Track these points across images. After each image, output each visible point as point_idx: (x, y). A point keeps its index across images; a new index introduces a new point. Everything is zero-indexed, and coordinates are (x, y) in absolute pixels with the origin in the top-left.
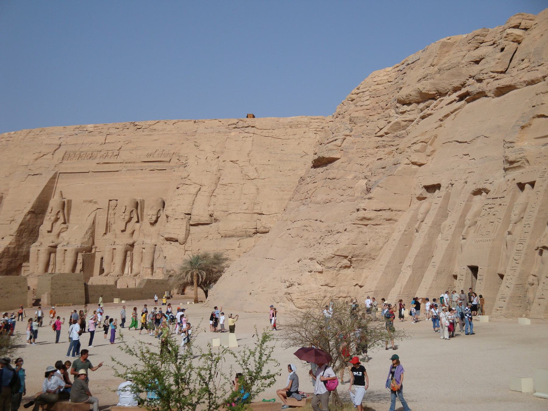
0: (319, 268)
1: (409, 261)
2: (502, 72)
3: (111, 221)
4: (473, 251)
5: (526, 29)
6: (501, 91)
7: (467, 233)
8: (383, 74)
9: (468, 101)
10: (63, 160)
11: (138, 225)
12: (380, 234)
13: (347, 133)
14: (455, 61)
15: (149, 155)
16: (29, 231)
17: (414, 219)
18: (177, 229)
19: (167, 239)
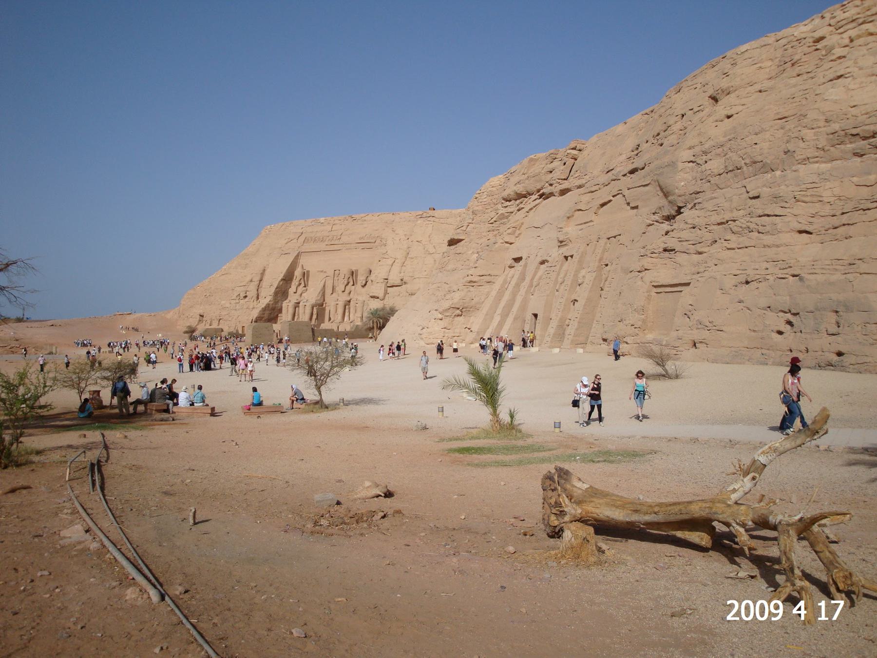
0: (440, 316)
1: (499, 311)
2: (566, 179)
3: (336, 284)
4: (536, 304)
6: (563, 192)
7: (534, 291)
8: (496, 180)
9: (545, 199)
13: (470, 221)
14: (537, 171)
15: (360, 239)
16: (282, 293)
17: (505, 282)
18: (378, 290)
19: (372, 297)
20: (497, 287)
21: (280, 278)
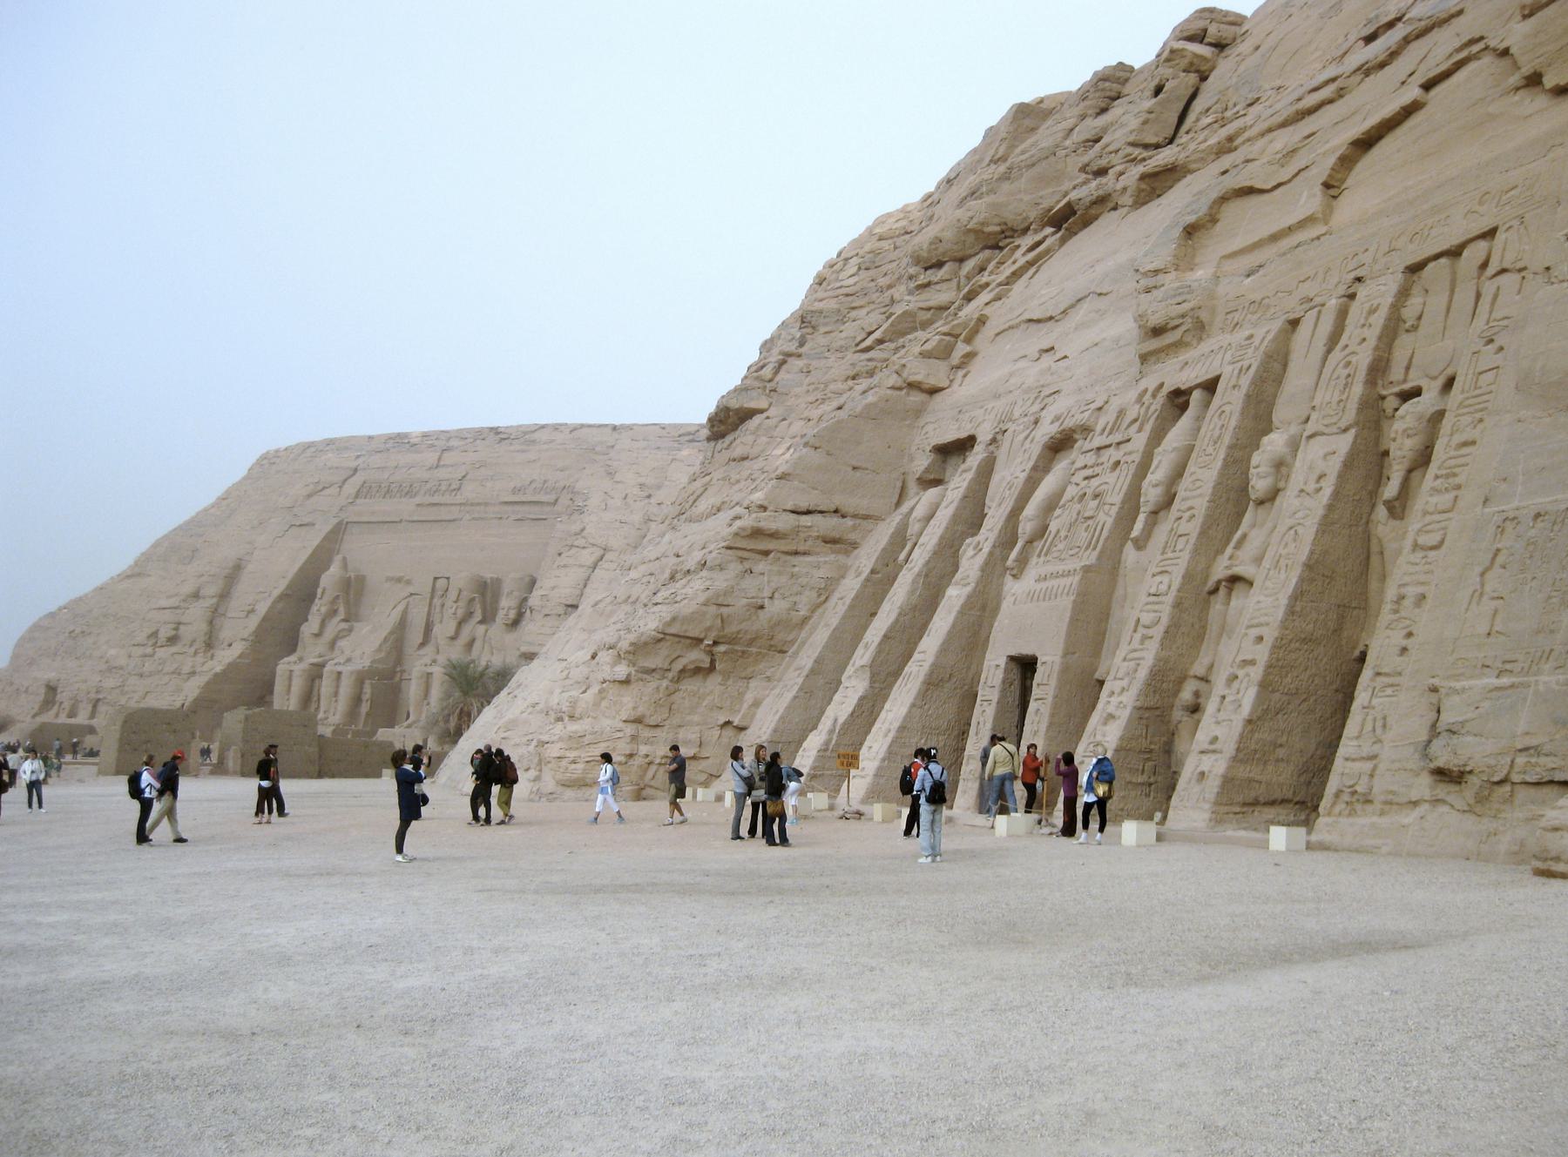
0: (622, 671)
1: (863, 656)
3: (436, 617)
5: (1220, 46)
10: (357, 497)
11: (482, 628)
12: (804, 581)
13: (792, 347)
15: (515, 491)
16: (281, 632)
20: (866, 558)
21: (276, 593)
